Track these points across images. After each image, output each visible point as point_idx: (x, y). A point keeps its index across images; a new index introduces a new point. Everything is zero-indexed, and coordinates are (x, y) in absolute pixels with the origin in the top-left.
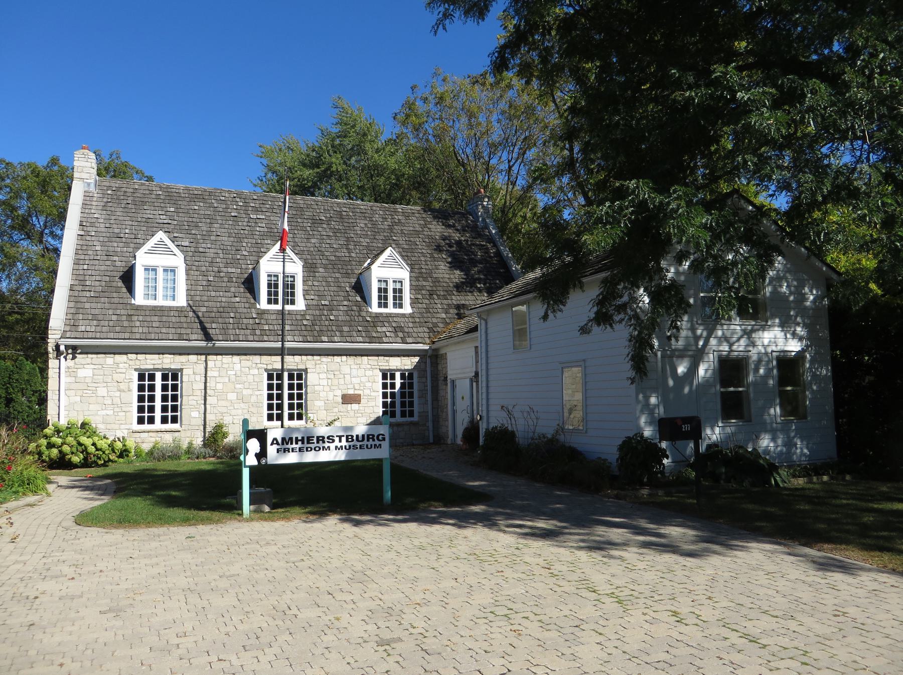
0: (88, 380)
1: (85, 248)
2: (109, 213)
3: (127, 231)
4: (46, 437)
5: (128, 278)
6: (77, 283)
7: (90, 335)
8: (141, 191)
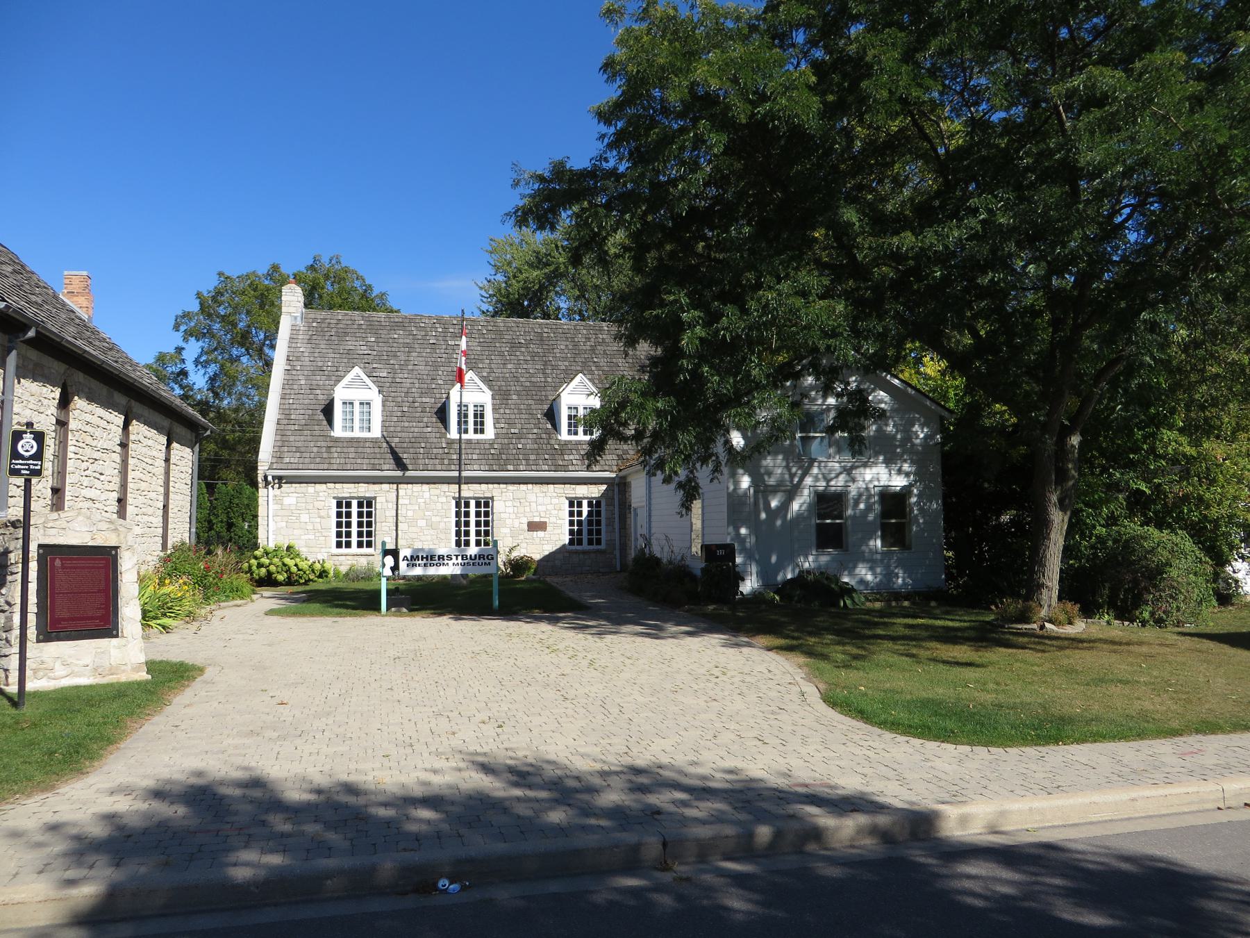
0: (293, 508)
4: (256, 558)
5: (328, 411)
7: (294, 466)
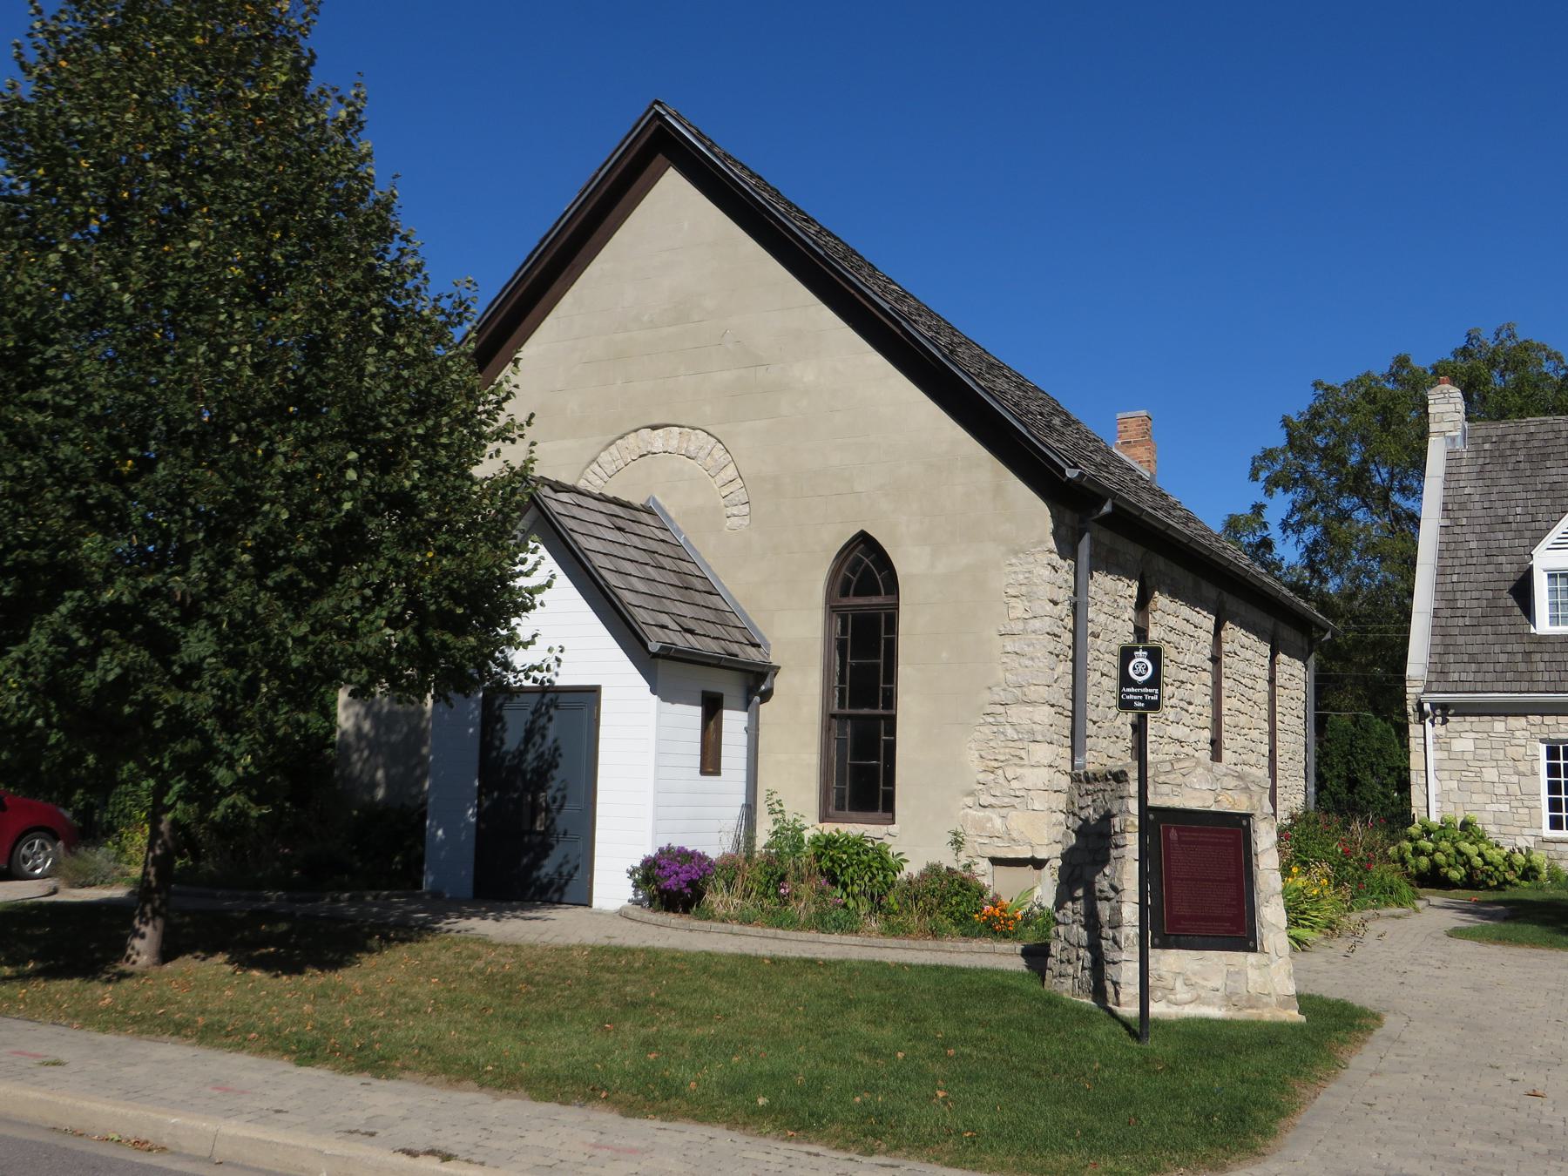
0: (1468, 756)
1: (1452, 546)
2: (1489, 482)
3: (1519, 510)
4: (1411, 840)
5: (1523, 591)
6: (1443, 604)
7: (1467, 687)
8: (1541, 436)
